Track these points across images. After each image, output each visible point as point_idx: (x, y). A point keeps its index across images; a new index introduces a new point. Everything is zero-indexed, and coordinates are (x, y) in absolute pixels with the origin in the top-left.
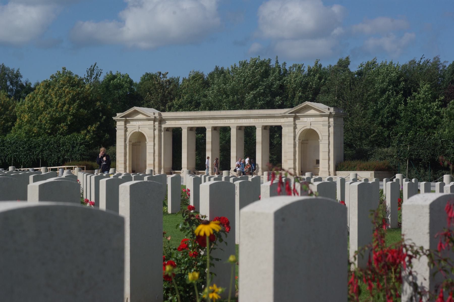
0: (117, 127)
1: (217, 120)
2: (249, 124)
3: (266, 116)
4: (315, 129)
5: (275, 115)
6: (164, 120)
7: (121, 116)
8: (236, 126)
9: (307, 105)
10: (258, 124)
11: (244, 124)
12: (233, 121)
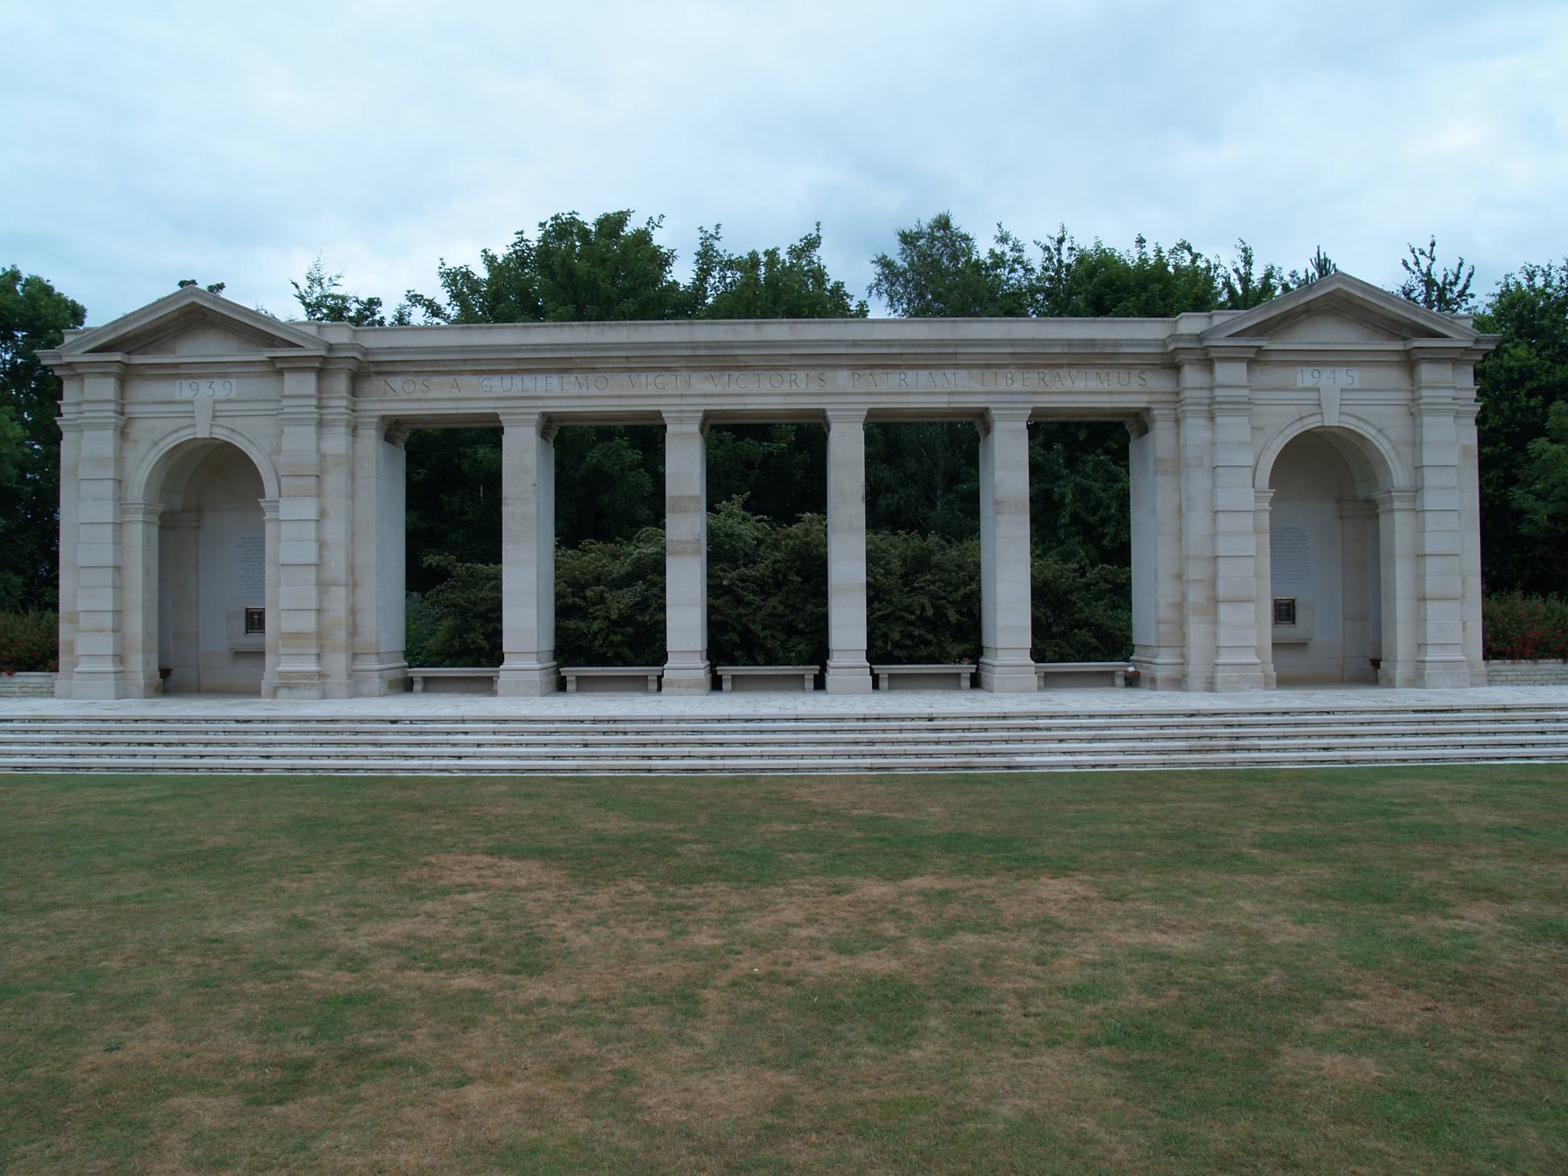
0: (63, 410)
1: (737, 374)
2: (945, 398)
3: (1066, 350)
4: (1367, 431)
5: (1122, 350)
6: (379, 373)
7: (87, 348)
8: (868, 407)
9: (1339, 289)
10: (1007, 398)
11: (912, 399)
12: (842, 379)
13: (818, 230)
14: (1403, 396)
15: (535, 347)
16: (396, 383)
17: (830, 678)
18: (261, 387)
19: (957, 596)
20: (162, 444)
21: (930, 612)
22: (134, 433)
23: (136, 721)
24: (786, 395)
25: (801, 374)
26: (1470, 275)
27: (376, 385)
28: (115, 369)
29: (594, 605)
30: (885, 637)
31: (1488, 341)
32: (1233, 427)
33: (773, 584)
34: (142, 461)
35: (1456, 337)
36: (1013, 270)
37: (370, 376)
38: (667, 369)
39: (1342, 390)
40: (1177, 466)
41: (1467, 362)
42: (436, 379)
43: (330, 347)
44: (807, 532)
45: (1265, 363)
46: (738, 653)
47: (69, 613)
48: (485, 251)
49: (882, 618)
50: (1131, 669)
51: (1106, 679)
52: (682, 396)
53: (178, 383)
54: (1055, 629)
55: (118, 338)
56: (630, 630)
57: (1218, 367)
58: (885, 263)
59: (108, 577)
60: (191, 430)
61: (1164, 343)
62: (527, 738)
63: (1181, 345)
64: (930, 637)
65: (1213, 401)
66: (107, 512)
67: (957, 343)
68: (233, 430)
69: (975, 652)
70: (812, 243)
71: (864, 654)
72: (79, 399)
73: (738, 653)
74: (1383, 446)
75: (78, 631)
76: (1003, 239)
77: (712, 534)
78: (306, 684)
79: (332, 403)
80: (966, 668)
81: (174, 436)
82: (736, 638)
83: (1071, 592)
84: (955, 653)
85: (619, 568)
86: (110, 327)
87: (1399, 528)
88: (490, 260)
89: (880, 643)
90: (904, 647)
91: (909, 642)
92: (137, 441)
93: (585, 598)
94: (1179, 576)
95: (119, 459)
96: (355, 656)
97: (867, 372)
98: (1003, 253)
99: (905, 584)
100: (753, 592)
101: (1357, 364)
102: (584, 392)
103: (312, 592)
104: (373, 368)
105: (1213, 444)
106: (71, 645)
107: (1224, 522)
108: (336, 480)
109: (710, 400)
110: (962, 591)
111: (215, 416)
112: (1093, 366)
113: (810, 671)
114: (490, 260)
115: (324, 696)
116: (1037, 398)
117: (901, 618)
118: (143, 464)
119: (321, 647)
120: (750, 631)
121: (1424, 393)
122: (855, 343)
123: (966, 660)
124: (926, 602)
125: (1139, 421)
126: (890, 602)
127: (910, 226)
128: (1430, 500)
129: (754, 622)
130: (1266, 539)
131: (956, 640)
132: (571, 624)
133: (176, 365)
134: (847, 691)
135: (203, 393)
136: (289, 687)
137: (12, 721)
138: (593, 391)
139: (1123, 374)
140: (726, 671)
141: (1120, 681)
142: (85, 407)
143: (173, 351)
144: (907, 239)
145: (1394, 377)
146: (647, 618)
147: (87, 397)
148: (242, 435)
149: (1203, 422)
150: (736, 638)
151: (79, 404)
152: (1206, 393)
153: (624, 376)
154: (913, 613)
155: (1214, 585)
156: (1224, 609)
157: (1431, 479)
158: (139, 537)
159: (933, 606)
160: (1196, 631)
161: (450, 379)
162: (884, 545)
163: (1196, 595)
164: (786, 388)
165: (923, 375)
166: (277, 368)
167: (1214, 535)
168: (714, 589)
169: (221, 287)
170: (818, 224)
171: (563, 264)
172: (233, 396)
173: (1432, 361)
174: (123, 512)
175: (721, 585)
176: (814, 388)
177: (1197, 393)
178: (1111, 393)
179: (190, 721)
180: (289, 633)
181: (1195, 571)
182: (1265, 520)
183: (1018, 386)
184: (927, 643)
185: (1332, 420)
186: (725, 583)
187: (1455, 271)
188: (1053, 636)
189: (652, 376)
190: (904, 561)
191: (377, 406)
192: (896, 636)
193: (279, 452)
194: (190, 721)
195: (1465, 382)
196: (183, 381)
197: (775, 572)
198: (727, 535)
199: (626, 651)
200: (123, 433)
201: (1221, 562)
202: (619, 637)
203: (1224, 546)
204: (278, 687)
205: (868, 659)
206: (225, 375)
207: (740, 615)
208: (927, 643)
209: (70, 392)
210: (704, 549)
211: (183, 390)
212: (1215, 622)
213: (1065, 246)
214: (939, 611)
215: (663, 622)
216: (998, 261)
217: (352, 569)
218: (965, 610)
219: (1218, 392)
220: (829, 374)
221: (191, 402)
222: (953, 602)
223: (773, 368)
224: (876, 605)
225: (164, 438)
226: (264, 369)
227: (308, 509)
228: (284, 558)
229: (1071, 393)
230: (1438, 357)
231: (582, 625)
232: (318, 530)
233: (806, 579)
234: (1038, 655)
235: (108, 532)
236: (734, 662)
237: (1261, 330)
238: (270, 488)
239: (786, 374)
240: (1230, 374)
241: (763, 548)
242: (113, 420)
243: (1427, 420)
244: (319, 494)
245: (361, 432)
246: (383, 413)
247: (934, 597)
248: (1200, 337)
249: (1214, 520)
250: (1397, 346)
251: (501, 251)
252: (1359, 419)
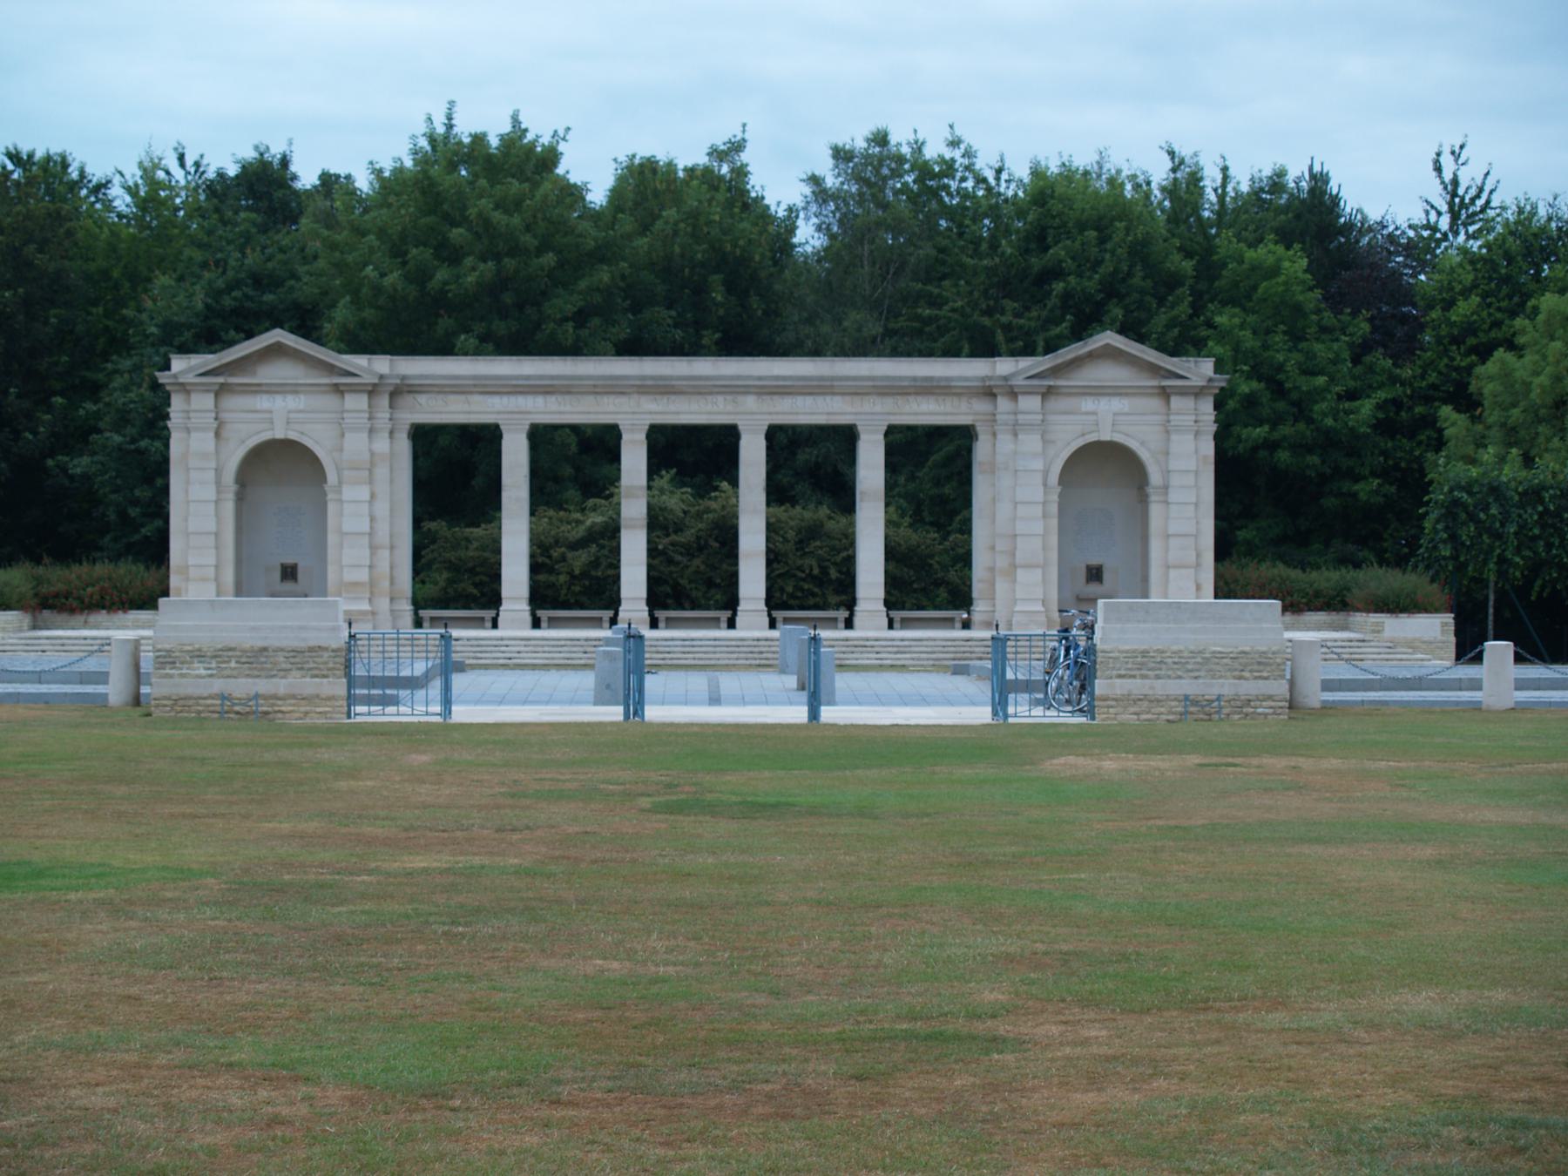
0: (172, 415)
2: (825, 417)
4: (1133, 444)
5: (953, 384)
6: (409, 392)
9: (1107, 345)
12: (750, 402)
13: (744, 131)
14: (1159, 418)
15: (528, 377)
16: (422, 399)
17: (739, 620)
18: (330, 401)
19: (839, 559)
21: (816, 571)
22: (224, 434)
24: (710, 413)
25: (720, 398)
26: (1491, 192)
27: (407, 400)
28: (217, 387)
29: (557, 562)
30: (782, 590)
31: (1219, 380)
32: (1031, 442)
33: (697, 548)
35: (1194, 378)
36: (963, 179)
38: (623, 393)
39: (1115, 414)
40: (992, 469)
41: (1210, 394)
42: (452, 398)
43: (381, 377)
44: (723, 508)
45: (1058, 394)
46: (669, 601)
48: (371, 163)
49: (780, 576)
50: (965, 616)
51: (948, 623)
52: (634, 413)
54: (915, 586)
56: (587, 583)
57: (1020, 397)
58: (815, 180)
59: (211, 540)
61: (983, 379)
62: (546, 649)
63: (992, 383)
64: (816, 590)
65: (1016, 424)
66: (211, 493)
67: (833, 379)
69: (850, 604)
70: (737, 146)
71: (763, 602)
72: (186, 407)
73: (669, 601)
74: (1144, 455)
75: (187, 579)
76: (954, 143)
77: (650, 508)
79: (379, 415)
80: (842, 614)
82: (669, 590)
83: (932, 556)
84: (833, 602)
85: (580, 532)
87: (1155, 511)
88: (378, 173)
89: (778, 595)
90: (797, 598)
91: (799, 594)
93: (550, 557)
94: (993, 548)
95: (217, 451)
96: (392, 599)
97: (768, 397)
98: (953, 160)
99: (797, 550)
100: (681, 554)
101: (1127, 395)
102: (562, 408)
103: (367, 552)
105: (1015, 453)
107: (1021, 511)
108: (382, 472)
109: (654, 416)
110: (844, 554)
111: (288, 423)
112: (933, 394)
113: (724, 615)
114: (378, 173)
116: (892, 417)
117: (794, 576)
118: (234, 457)
119: (372, 593)
120: (679, 584)
121: (1172, 417)
122: (760, 378)
123: (842, 608)
124: (814, 563)
125: (964, 437)
126: (786, 563)
127: (843, 140)
128: (1173, 496)
129: (682, 577)
130: (1054, 522)
131: (837, 592)
132: (542, 577)
134: (750, 628)
135: (280, 405)
138: (568, 408)
139: (955, 399)
140: (661, 614)
141: (958, 625)
143: (254, 374)
144: (841, 155)
145: (1155, 403)
146: (600, 574)
149: (1009, 437)
150: (669, 590)
151: (188, 412)
152: (1012, 417)
153: (591, 398)
154: (803, 572)
155: (1014, 555)
156: (1019, 571)
157: (1175, 480)
158: (229, 507)
159: (819, 566)
160: (1001, 587)
161: (462, 398)
162: (784, 516)
163: (1002, 562)
164: (709, 408)
165: (809, 400)
166: (338, 390)
167: (1014, 519)
168: (652, 552)
170: (744, 125)
171: (480, 215)
172: (302, 407)
173: (1176, 394)
174: (218, 492)
175: (656, 549)
176: (730, 408)
177: (1005, 417)
178: (946, 414)
181: (1001, 545)
182: (1054, 509)
183: (878, 408)
184: (814, 595)
185: (1106, 436)
186: (660, 547)
187: (1479, 183)
188: (915, 591)
189: (611, 398)
190: (799, 532)
191: (409, 416)
192: (790, 589)
193: (341, 450)
195: (1207, 406)
197: (698, 538)
198: (661, 509)
199: (584, 599)
200: (217, 434)
201: (1019, 539)
202: (577, 589)
203: (1020, 528)
205: (767, 604)
206: (296, 392)
207: (671, 573)
208: (814, 595)
209: (177, 404)
210: (645, 523)
211: (263, 402)
212: (1014, 581)
213: (1004, 176)
214: (824, 571)
215: (618, 577)
216: (949, 167)
217: (391, 536)
218: (845, 569)
219: (1020, 417)
220: (740, 398)
221: (271, 412)
222: (835, 564)
223: (700, 393)
224: (775, 565)
227: (363, 493)
228: (347, 526)
229: (916, 414)
230: (1183, 392)
231: (552, 578)
233: (723, 544)
234: (890, 604)
235: (212, 506)
236: (665, 607)
237: (1055, 371)
238: (332, 477)
239: (709, 398)
240: (1030, 403)
241: (687, 519)
243: (1174, 437)
244: (371, 482)
245: (397, 435)
247: (821, 560)
248: (1005, 378)
249: (1015, 508)
250: (1155, 383)
251: (387, 166)
252: (1127, 435)
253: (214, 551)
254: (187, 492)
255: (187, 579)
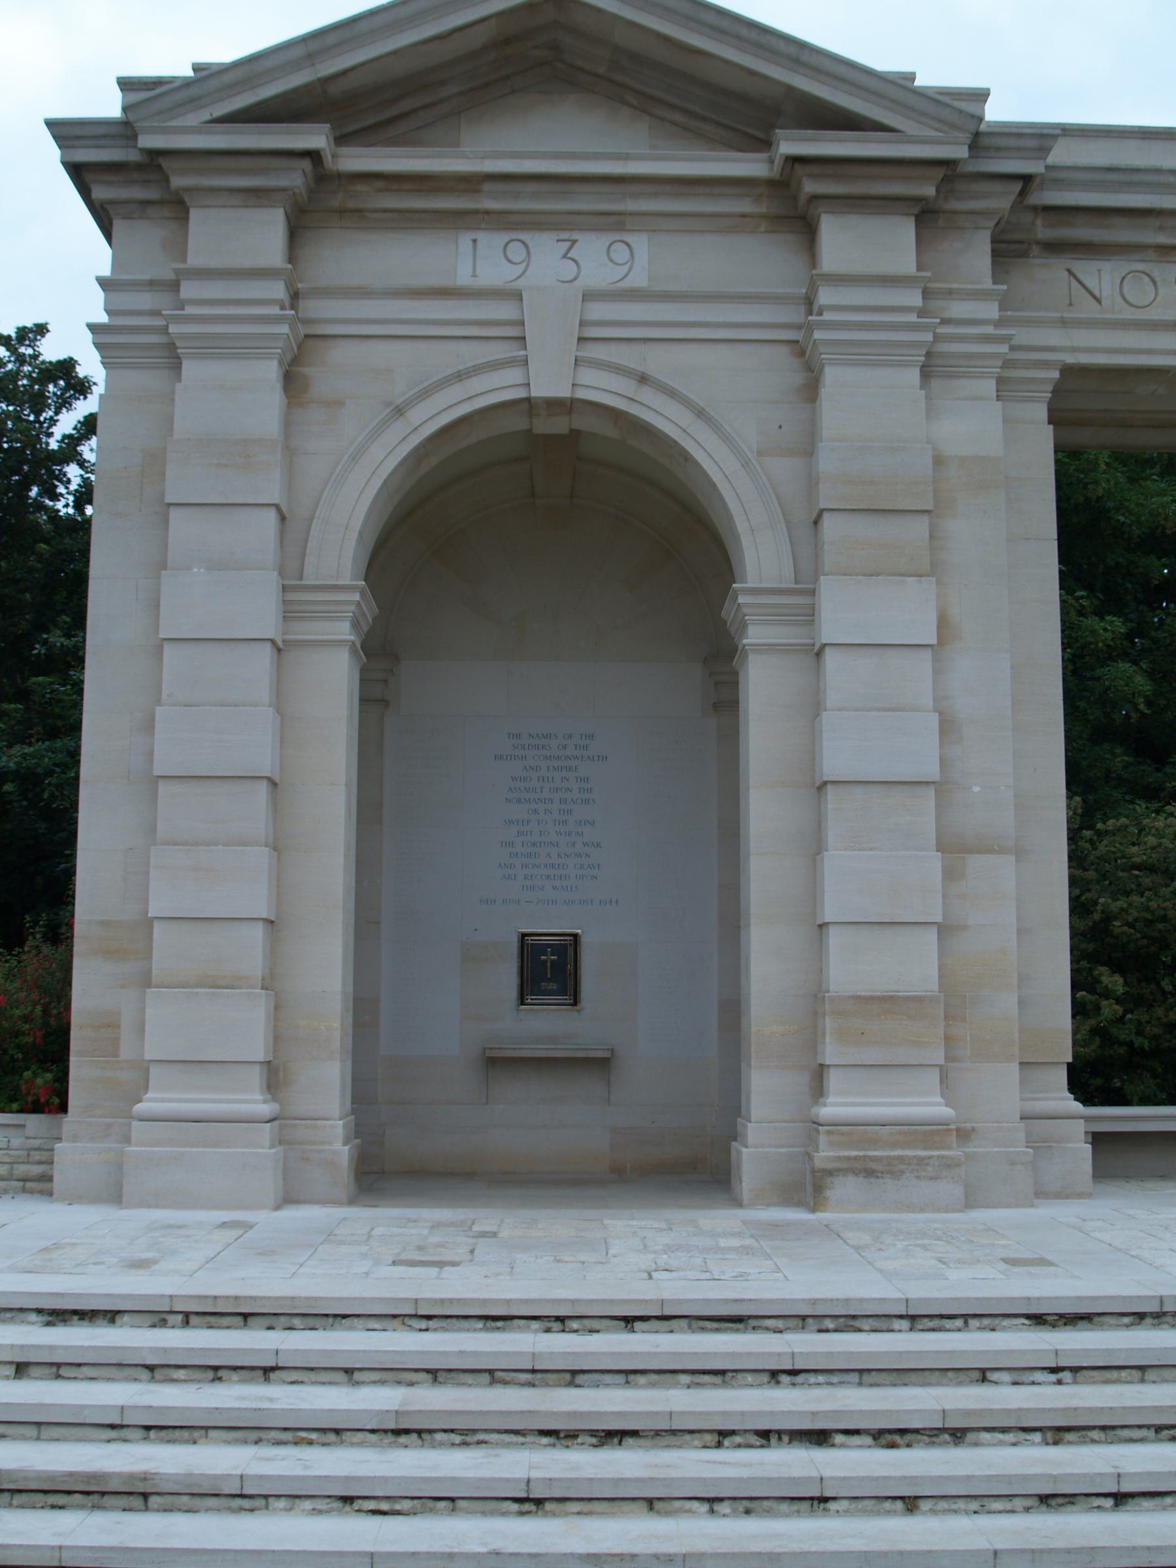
6: (1055, 248)
20: (416, 415)
23: (629, 1322)
34: (354, 459)
37: (1024, 255)
47: (105, 924)
53: (465, 240)
55: (307, 88)
60: (513, 375)
68: (643, 379)
75: (146, 982)
78: (921, 1161)
79: (959, 309)
81: (455, 392)
86: (300, 52)
92: (338, 403)
103: (934, 864)
104: (1043, 231)
106: (110, 1024)
111: (581, 339)
115: (970, 1202)
133: (470, 183)
136: (867, 1171)
137: (111, 1316)
142: (189, 290)
147: (195, 259)
148: (672, 393)
169: (41, 330)
172: (638, 279)
174: (289, 613)
179: (849, 1322)
180: (858, 998)
194: (849, 1322)
196: (483, 237)
204: (830, 1173)
206: (614, 222)
221: (518, 296)
225: (426, 393)
226: (745, 206)
232: (938, 672)
242: (285, 329)
246: (1070, 359)
253: (260, 856)
254: (156, 605)
255: (146, 982)
